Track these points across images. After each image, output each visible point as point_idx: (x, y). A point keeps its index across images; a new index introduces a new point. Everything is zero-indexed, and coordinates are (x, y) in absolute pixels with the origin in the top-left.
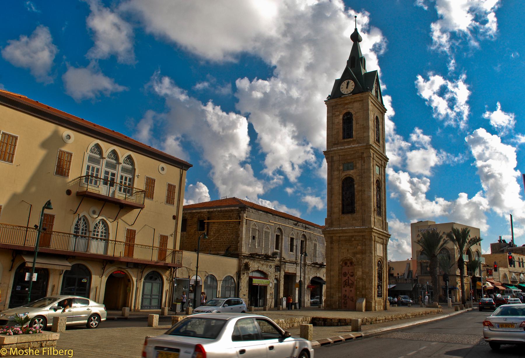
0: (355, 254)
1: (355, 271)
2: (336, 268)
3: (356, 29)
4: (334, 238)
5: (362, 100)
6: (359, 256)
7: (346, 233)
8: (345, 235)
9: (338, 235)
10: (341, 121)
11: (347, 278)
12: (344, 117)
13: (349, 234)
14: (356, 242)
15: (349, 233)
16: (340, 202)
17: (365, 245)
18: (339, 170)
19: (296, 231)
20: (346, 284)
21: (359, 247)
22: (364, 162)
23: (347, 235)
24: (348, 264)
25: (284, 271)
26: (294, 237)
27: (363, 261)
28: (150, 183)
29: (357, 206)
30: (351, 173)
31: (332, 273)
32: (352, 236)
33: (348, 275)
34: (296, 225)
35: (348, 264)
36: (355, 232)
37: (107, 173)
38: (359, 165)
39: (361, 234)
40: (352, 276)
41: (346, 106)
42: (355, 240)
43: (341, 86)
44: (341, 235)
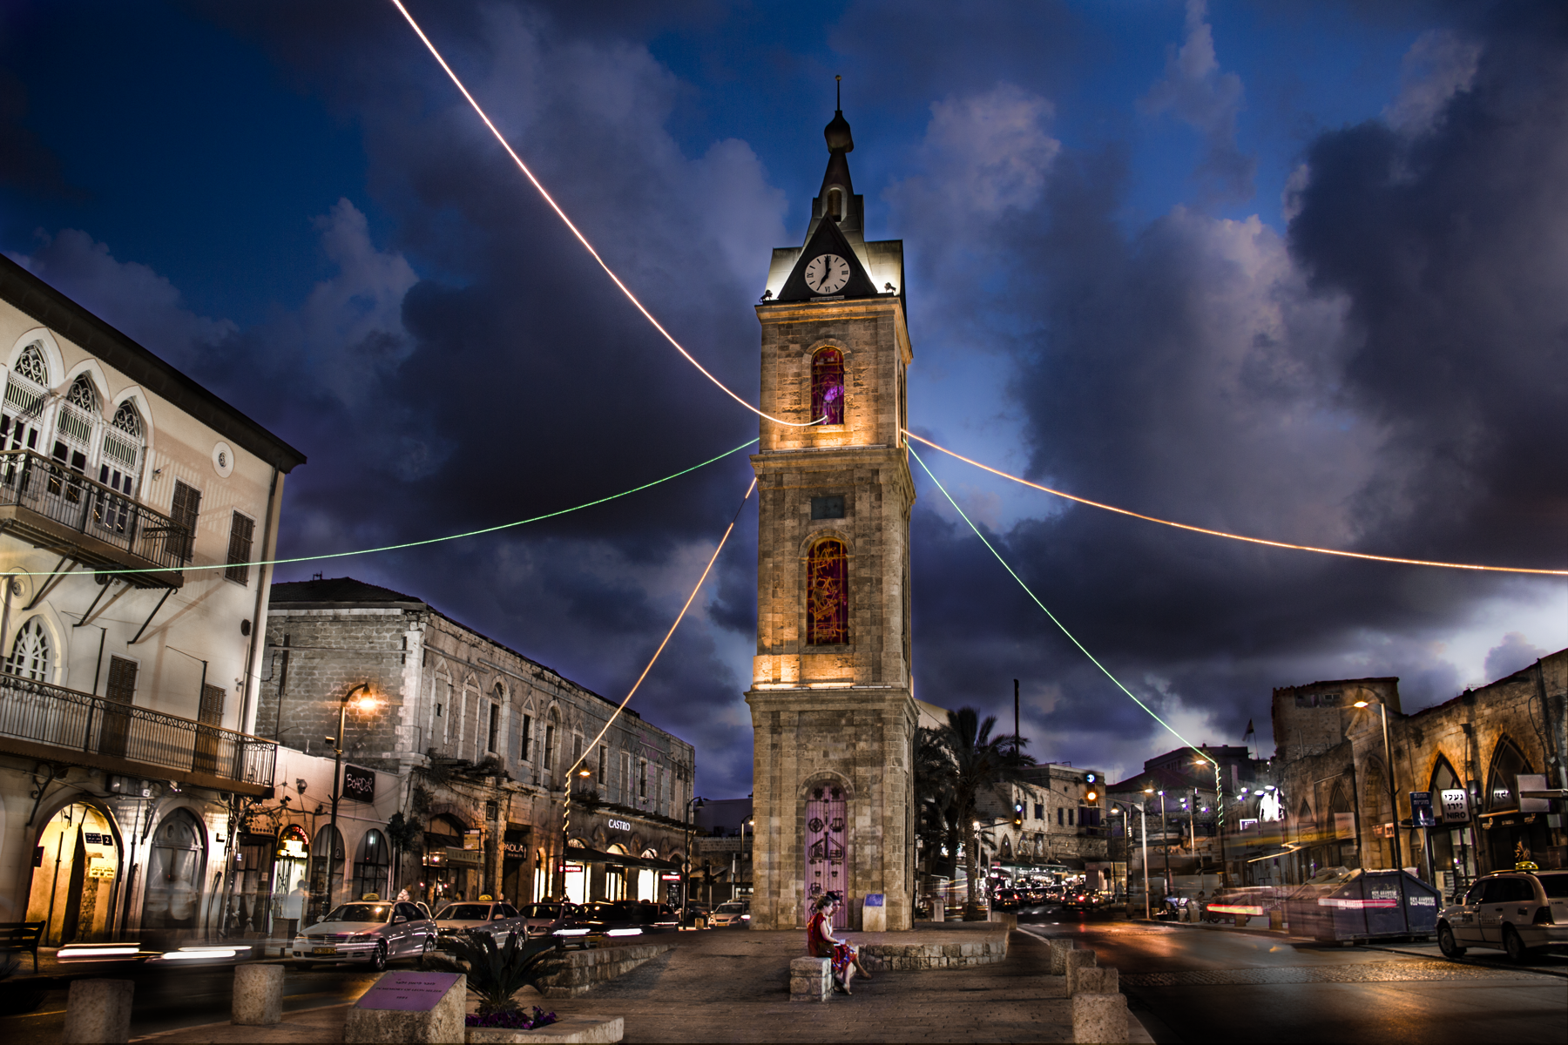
0: (848, 764)
1: (850, 815)
2: (790, 807)
3: (839, 113)
4: (783, 716)
5: (875, 320)
6: (861, 771)
7: (823, 702)
8: (818, 707)
9: (797, 708)
10: (808, 374)
11: (821, 835)
12: (815, 360)
13: (831, 707)
14: (850, 730)
15: (832, 701)
16: (804, 611)
17: (882, 739)
18: (795, 514)
19: (539, 696)
20: (820, 852)
21: (862, 745)
22: (879, 497)
23: (824, 707)
24: (827, 795)
25: (506, 818)
26: (532, 713)
27: (876, 787)
28: (187, 499)
29: (856, 627)
31: (776, 822)
32: (841, 714)
33: (826, 828)
34: (539, 676)
36: (851, 699)
38: (863, 505)
39: (870, 706)
40: (837, 830)
41: (823, 331)
42: (850, 723)
43: (808, 270)
44: (808, 707)
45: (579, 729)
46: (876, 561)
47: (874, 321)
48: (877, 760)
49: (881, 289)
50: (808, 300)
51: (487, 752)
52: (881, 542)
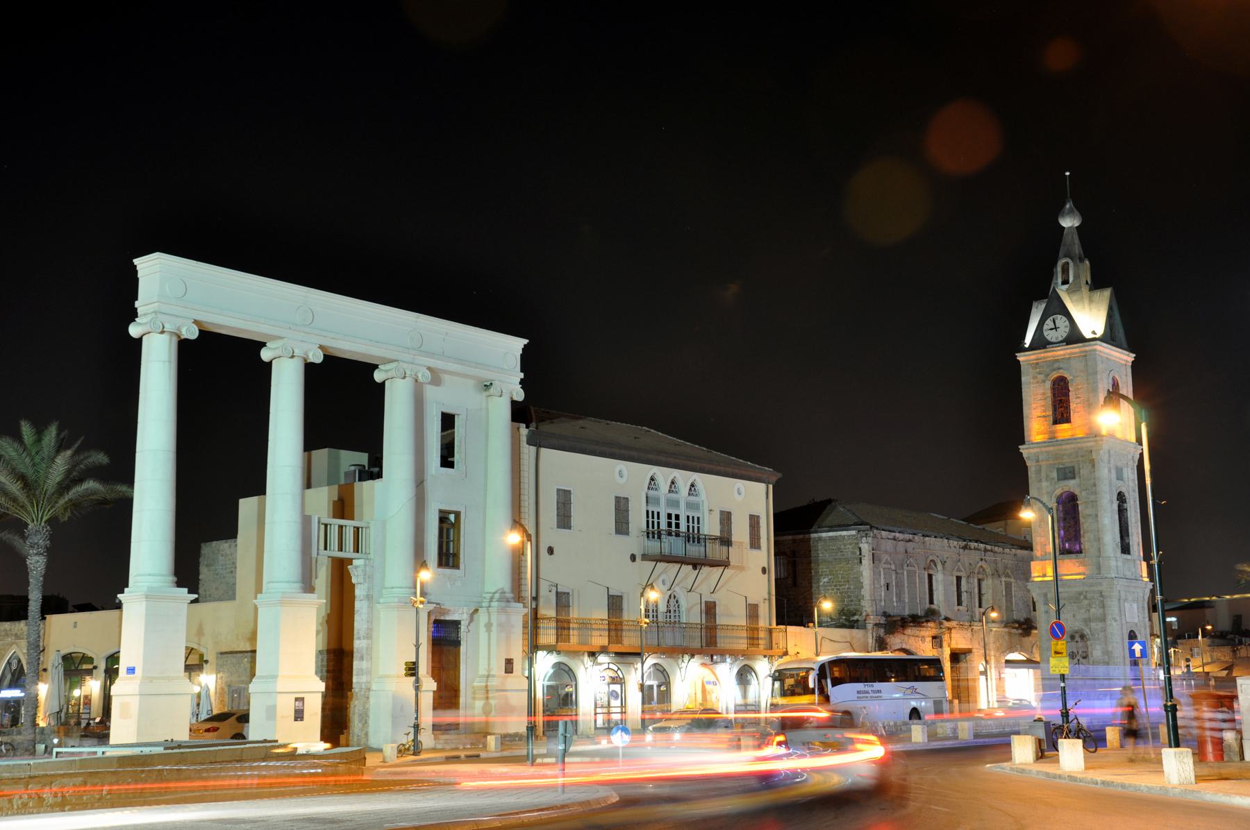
0: (1087, 621)
6: (1093, 625)
10: (1049, 393)
14: (1086, 602)
17: (1104, 607)
21: (1093, 610)
22: (1093, 466)
24: (1078, 638)
28: (726, 518)
29: (1087, 541)
30: (1072, 485)
32: (1080, 594)
35: (1078, 638)
37: (669, 516)
39: (1095, 589)
40: (1084, 658)
42: (1085, 598)
45: (1007, 576)
46: (1094, 504)
47: (1084, 356)
48: (1103, 619)
49: (1088, 335)
50: (1045, 347)
51: (928, 605)
52: (1096, 493)
